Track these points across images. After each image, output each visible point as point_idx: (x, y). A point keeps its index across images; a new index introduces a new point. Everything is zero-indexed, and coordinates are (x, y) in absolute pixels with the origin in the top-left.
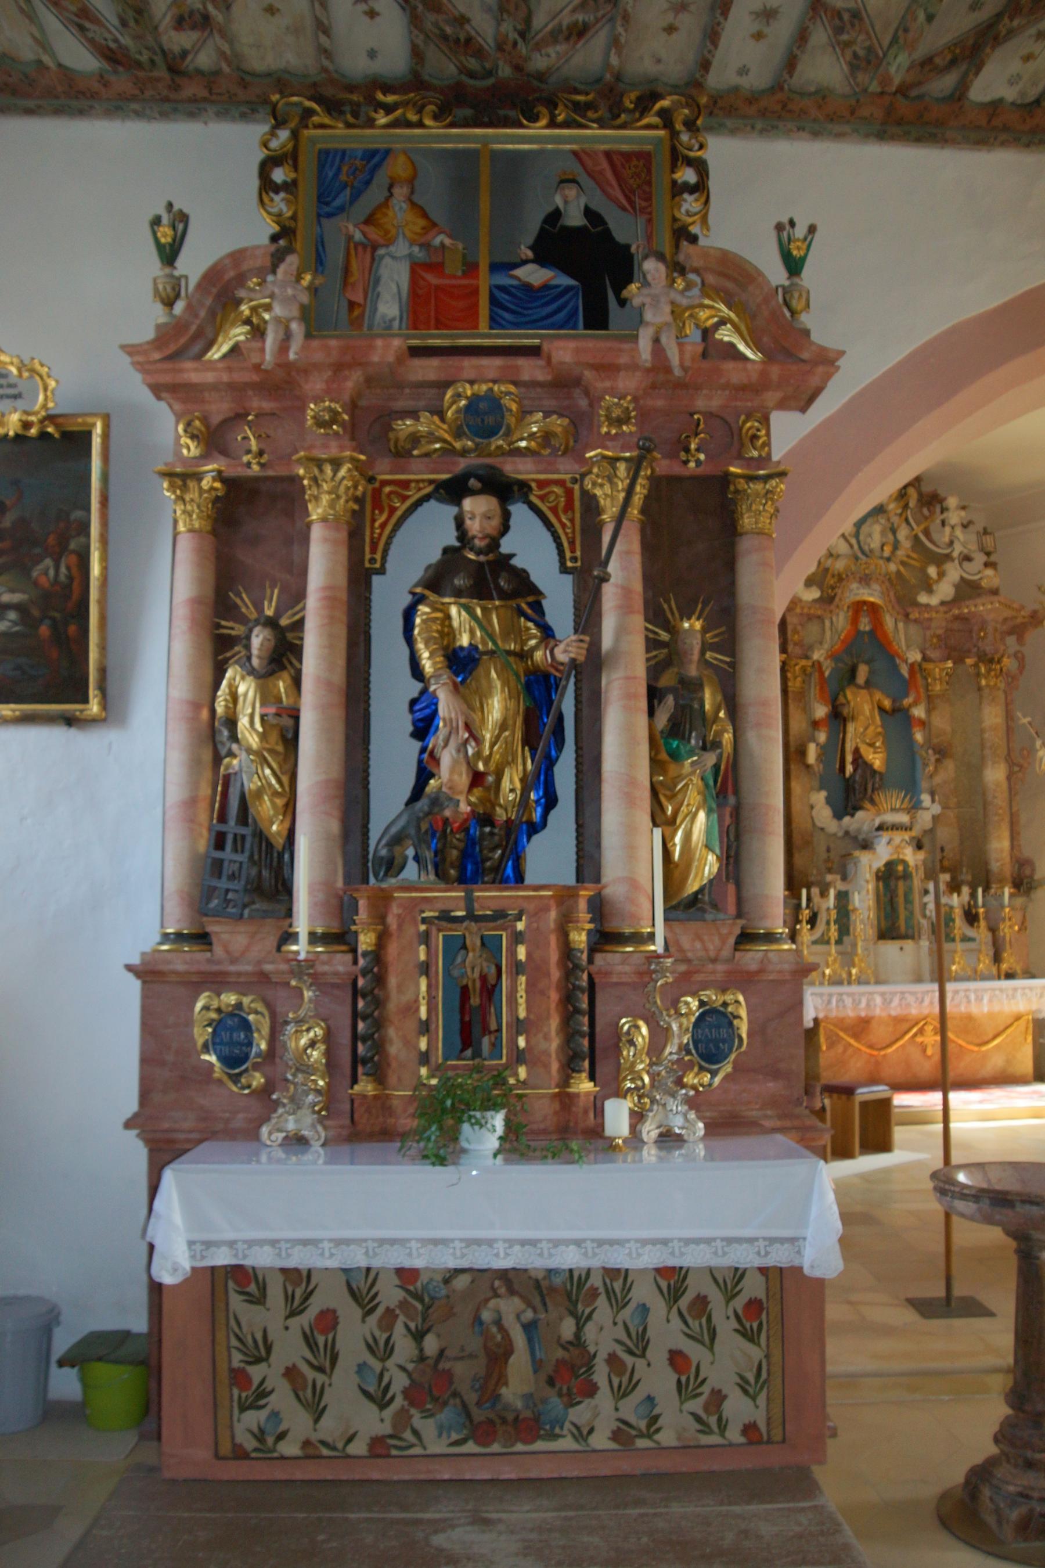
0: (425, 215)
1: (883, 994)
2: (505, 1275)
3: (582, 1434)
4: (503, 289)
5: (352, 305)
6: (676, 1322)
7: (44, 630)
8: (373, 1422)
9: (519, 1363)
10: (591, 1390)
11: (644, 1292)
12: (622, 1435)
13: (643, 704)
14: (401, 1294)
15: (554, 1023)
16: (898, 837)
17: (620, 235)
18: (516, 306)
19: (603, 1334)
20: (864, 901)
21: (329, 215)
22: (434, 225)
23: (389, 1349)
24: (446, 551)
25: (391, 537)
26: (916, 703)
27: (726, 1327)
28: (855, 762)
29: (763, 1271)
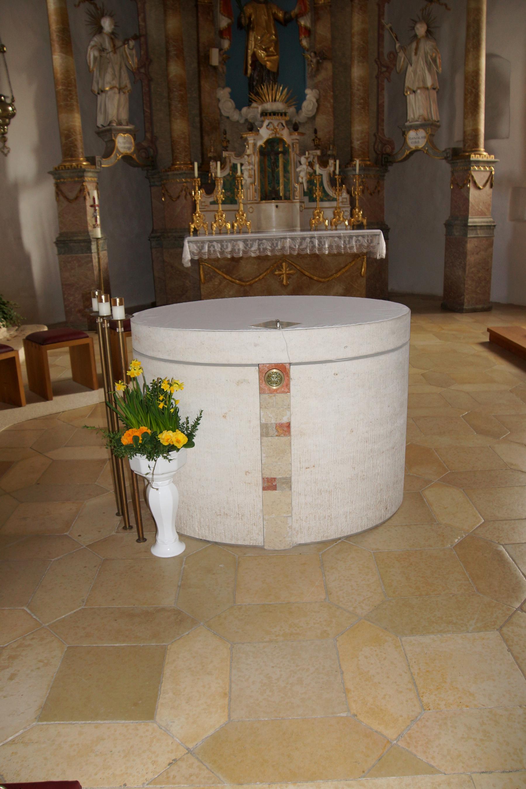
1: (245, 241)
16: (276, 121)
26: (301, 14)
28: (254, 64)
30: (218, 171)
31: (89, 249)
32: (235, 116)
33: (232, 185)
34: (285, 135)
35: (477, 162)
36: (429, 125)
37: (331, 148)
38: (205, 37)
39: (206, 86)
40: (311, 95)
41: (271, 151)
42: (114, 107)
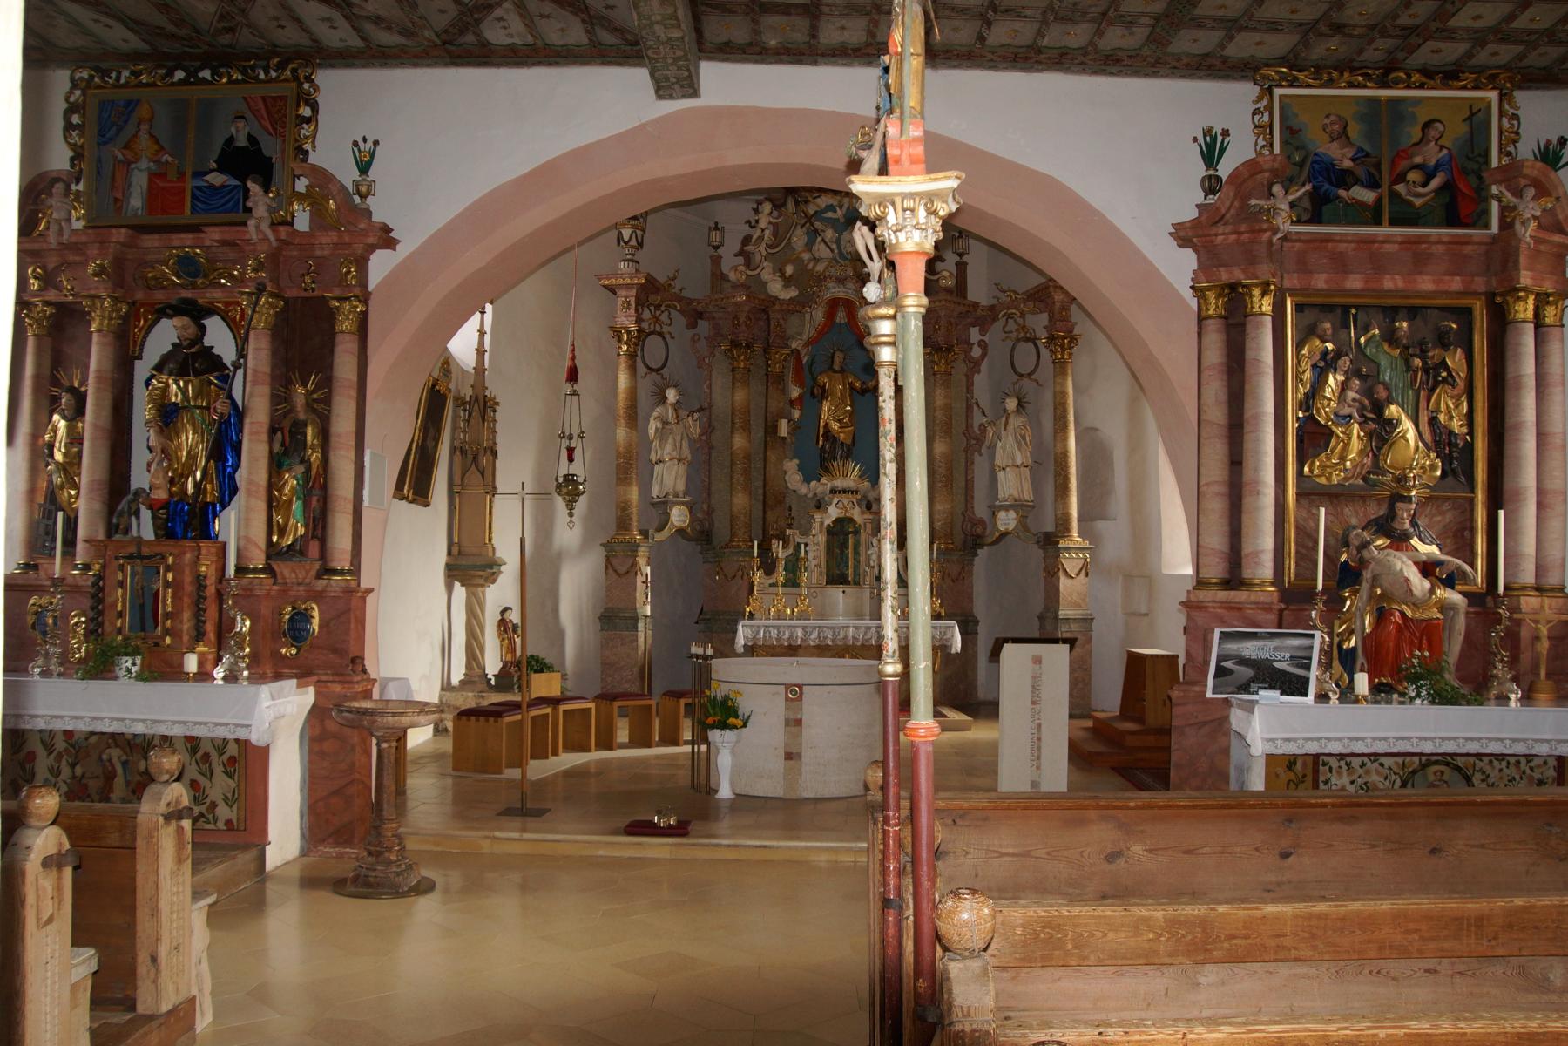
0: (157, 142)
1: (804, 628)
2: (113, 735)
4: (198, 188)
5: (116, 200)
6: (194, 766)
13: (264, 437)
14: (64, 745)
15: (186, 615)
17: (267, 153)
18: (208, 198)
21: (105, 143)
22: (162, 148)
23: (59, 773)
24: (174, 345)
25: (145, 338)
27: (218, 769)
29: (237, 741)
30: (780, 551)
31: (635, 628)
32: (803, 490)
33: (794, 566)
34: (856, 514)
35: (1068, 549)
36: (1017, 505)
39: (772, 456)
42: (669, 477)
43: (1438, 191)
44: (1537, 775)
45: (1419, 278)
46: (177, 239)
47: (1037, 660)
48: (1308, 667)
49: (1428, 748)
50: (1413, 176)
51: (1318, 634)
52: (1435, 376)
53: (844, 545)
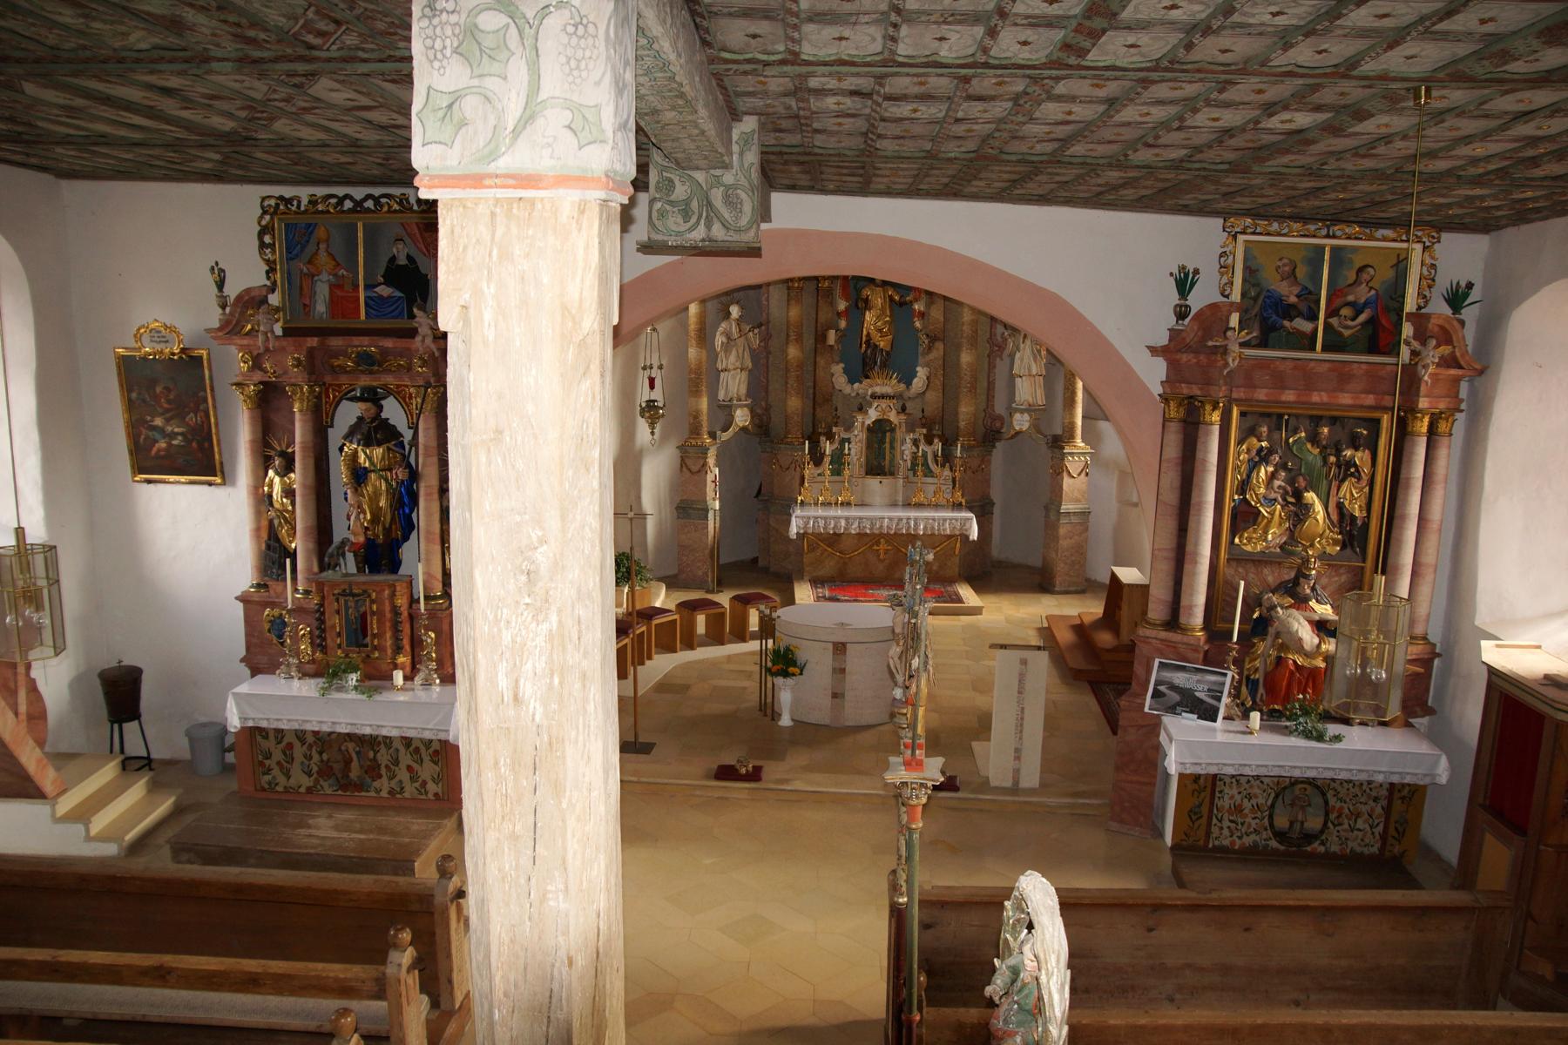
2: (348, 734)
3: (378, 791)
7: (194, 445)
8: (307, 782)
9: (355, 765)
10: (380, 776)
11: (397, 744)
12: (391, 792)
15: (388, 635)
16: (884, 404)
19: (383, 757)
20: (856, 451)
23: (311, 758)
26: (916, 300)
27: (426, 758)
30: (828, 448)
32: (847, 389)
34: (893, 417)
35: (1071, 454)
37: (939, 427)
38: (823, 317)
39: (821, 362)
40: (922, 372)
41: (879, 430)
42: (734, 384)
43: (1363, 324)
44: (1374, 794)
45: (1341, 395)
46: (356, 340)
47: (1024, 662)
48: (1219, 699)
49: (1297, 773)
50: (1345, 312)
51: (1230, 674)
52: (1347, 470)
53: (882, 442)
